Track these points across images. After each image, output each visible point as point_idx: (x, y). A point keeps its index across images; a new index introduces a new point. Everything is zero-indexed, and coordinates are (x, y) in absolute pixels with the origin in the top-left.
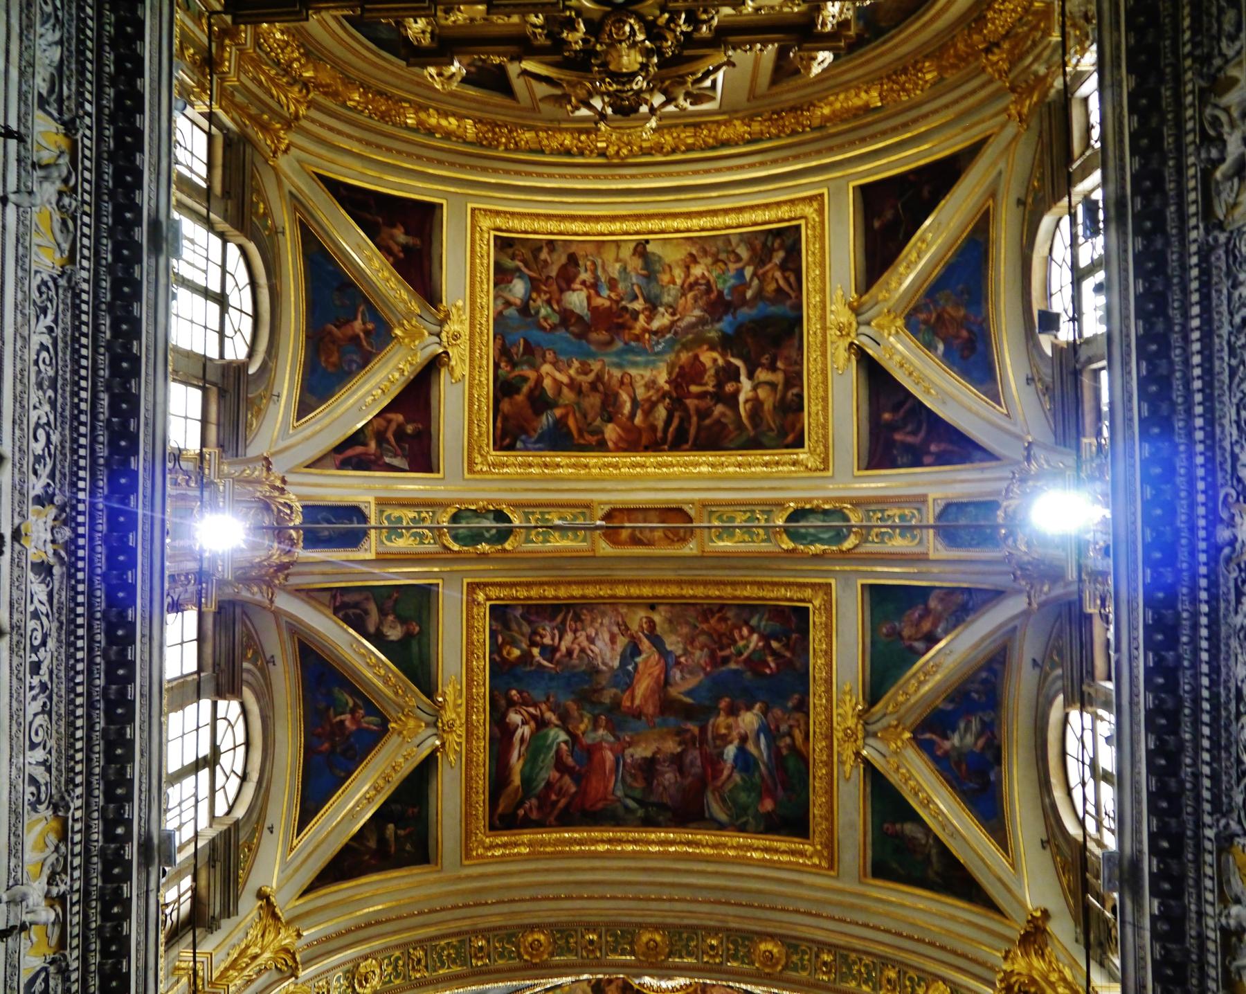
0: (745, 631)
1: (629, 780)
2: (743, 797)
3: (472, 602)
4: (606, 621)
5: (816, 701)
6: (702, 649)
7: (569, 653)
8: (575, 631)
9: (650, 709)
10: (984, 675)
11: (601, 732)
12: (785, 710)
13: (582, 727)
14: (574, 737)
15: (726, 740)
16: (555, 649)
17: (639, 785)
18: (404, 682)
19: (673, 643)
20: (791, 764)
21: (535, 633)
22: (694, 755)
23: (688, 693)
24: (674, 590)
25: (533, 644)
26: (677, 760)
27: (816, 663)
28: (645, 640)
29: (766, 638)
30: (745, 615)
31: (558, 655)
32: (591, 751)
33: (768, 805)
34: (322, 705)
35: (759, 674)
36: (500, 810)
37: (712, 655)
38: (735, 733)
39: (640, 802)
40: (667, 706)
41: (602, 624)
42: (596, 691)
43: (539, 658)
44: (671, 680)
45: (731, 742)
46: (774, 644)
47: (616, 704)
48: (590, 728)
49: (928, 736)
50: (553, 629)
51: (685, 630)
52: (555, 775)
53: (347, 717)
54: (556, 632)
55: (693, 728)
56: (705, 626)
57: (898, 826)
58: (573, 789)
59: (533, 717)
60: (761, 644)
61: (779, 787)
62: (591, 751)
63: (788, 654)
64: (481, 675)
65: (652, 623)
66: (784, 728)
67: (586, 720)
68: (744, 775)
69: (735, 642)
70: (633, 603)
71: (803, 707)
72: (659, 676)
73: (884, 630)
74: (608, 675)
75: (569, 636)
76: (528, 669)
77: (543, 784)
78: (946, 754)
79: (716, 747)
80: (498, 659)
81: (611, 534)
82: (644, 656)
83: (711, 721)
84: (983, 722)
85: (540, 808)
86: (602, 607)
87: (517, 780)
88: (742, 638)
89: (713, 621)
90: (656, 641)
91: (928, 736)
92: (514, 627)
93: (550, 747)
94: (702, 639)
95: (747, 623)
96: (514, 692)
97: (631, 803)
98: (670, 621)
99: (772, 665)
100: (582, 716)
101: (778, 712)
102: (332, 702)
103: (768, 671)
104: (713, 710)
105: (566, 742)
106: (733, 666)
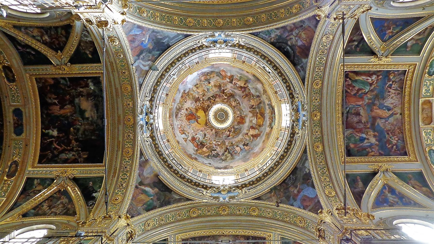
0: (397, 139)
1: (354, 109)
2: (353, 139)
3: (411, 65)
4: (397, 102)
5: (385, 158)
6: (390, 128)
7: (389, 92)
8: (395, 93)
9: (373, 114)
10: (412, 202)
11: (367, 101)
12: (378, 150)
13: (369, 96)
14: (367, 93)
15: (367, 134)
16: (390, 88)
17: (353, 111)
18: (397, 46)
19: (391, 120)
20: (364, 152)
21: (396, 82)
22: (362, 126)
23: (378, 123)
24: (407, 119)
25: (393, 82)
26: (360, 122)
27: (392, 158)
28: (392, 112)
29: (396, 145)
30: (401, 139)
31: (389, 89)
32: (362, 98)
33: (352, 146)
34: (398, 24)
35: (386, 143)
36: (350, 74)
37: (389, 130)
38: (369, 137)
39: (348, 112)
40: (374, 119)
41: (396, 100)
42: (378, 99)
43: (389, 83)
44: (381, 119)
45: (366, 136)
46: (395, 147)
47: (374, 105)
48: (368, 98)
49: (387, 187)
50: (396, 87)
51: (395, 123)
52: (357, 88)
53: (391, 30)
54: (395, 88)
55: (369, 126)
56: (396, 128)
57: (360, 180)
58: (352, 94)
59: (373, 82)
60: (394, 143)
61: (357, 149)
62: (362, 98)
63: (393, 150)
64: (389, 68)
65: (397, 114)
66: (373, 150)
67: (370, 97)
68: (358, 140)
69: (393, 136)
70: (403, 109)
71: (381, 155)
72: (382, 116)
73: (410, 176)
74: (382, 102)
75: (394, 92)
76: (386, 81)
77: (354, 85)
78: (384, 193)
79: (365, 132)
80: (391, 72)
81: (424, 103)
82: (388, 112)
83: (371, 130)
84: (397, 202)
85: (348, 85)
86: (401, 101)
87: (357, 78)
88: (394, 138)
89: (398, 130)
90: (392, 115)
91: (387, 187)
92: (398, 77)
93: (364, 87)
94: (393, 128)
95: (399, 139)
96: (381, 77)
97: (348, 109)
98: (397, 119)
99: (389, 146)
100: (372, 95)
101: (377, 148)
102: (397, 26)
103: (387, 145)
104: (374, 131)
105: (365, 91)
106: (387, 136)
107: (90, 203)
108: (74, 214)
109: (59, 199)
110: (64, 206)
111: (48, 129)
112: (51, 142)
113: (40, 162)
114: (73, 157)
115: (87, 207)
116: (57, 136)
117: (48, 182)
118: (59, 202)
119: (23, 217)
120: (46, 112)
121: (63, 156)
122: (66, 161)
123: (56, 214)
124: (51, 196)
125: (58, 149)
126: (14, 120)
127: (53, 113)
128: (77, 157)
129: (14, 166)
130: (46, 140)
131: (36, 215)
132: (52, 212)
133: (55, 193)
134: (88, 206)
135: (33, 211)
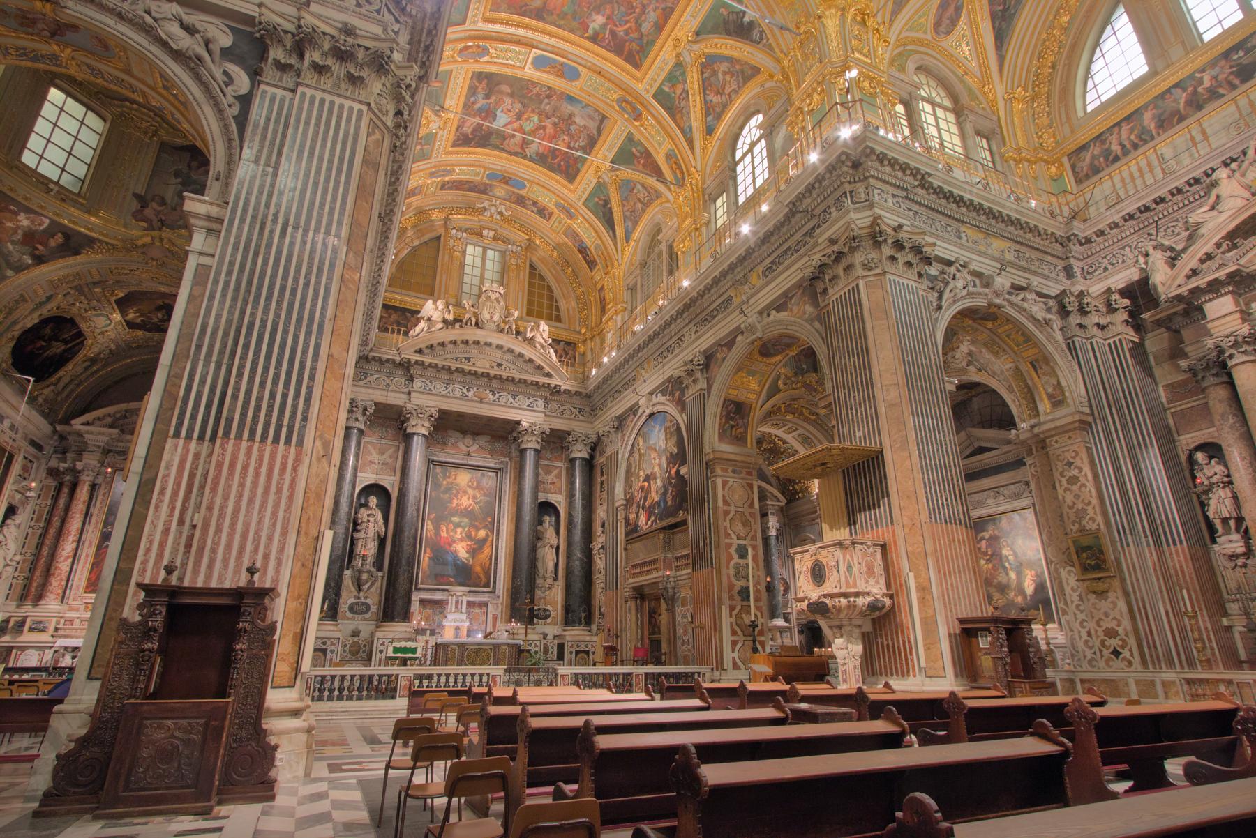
107: (755, 34)
108: (756, 71)
109: (714, 73)
110: (732, 75)
111: (588, 27)
112: (613, 33)
113: (637, 66)
114: (659, 12)
115: (760, 46)
116: (609, 18)
117: (678, 73)
118: (721, 76)
119: (710, 135)
120: (555, 17)
121: (646, 27)
122: (659, 27)
123: (736, 91)
124: (703, 82)
125: (630, 28)
126: (550, 72)
127: (563, 6)
128: (663, 6)
129: (624, 104)
130: (603, 38)
131: (719, 117)
132: (729, 94)
133: (702, 73)
134: (759, 43)
135: (708, 119)
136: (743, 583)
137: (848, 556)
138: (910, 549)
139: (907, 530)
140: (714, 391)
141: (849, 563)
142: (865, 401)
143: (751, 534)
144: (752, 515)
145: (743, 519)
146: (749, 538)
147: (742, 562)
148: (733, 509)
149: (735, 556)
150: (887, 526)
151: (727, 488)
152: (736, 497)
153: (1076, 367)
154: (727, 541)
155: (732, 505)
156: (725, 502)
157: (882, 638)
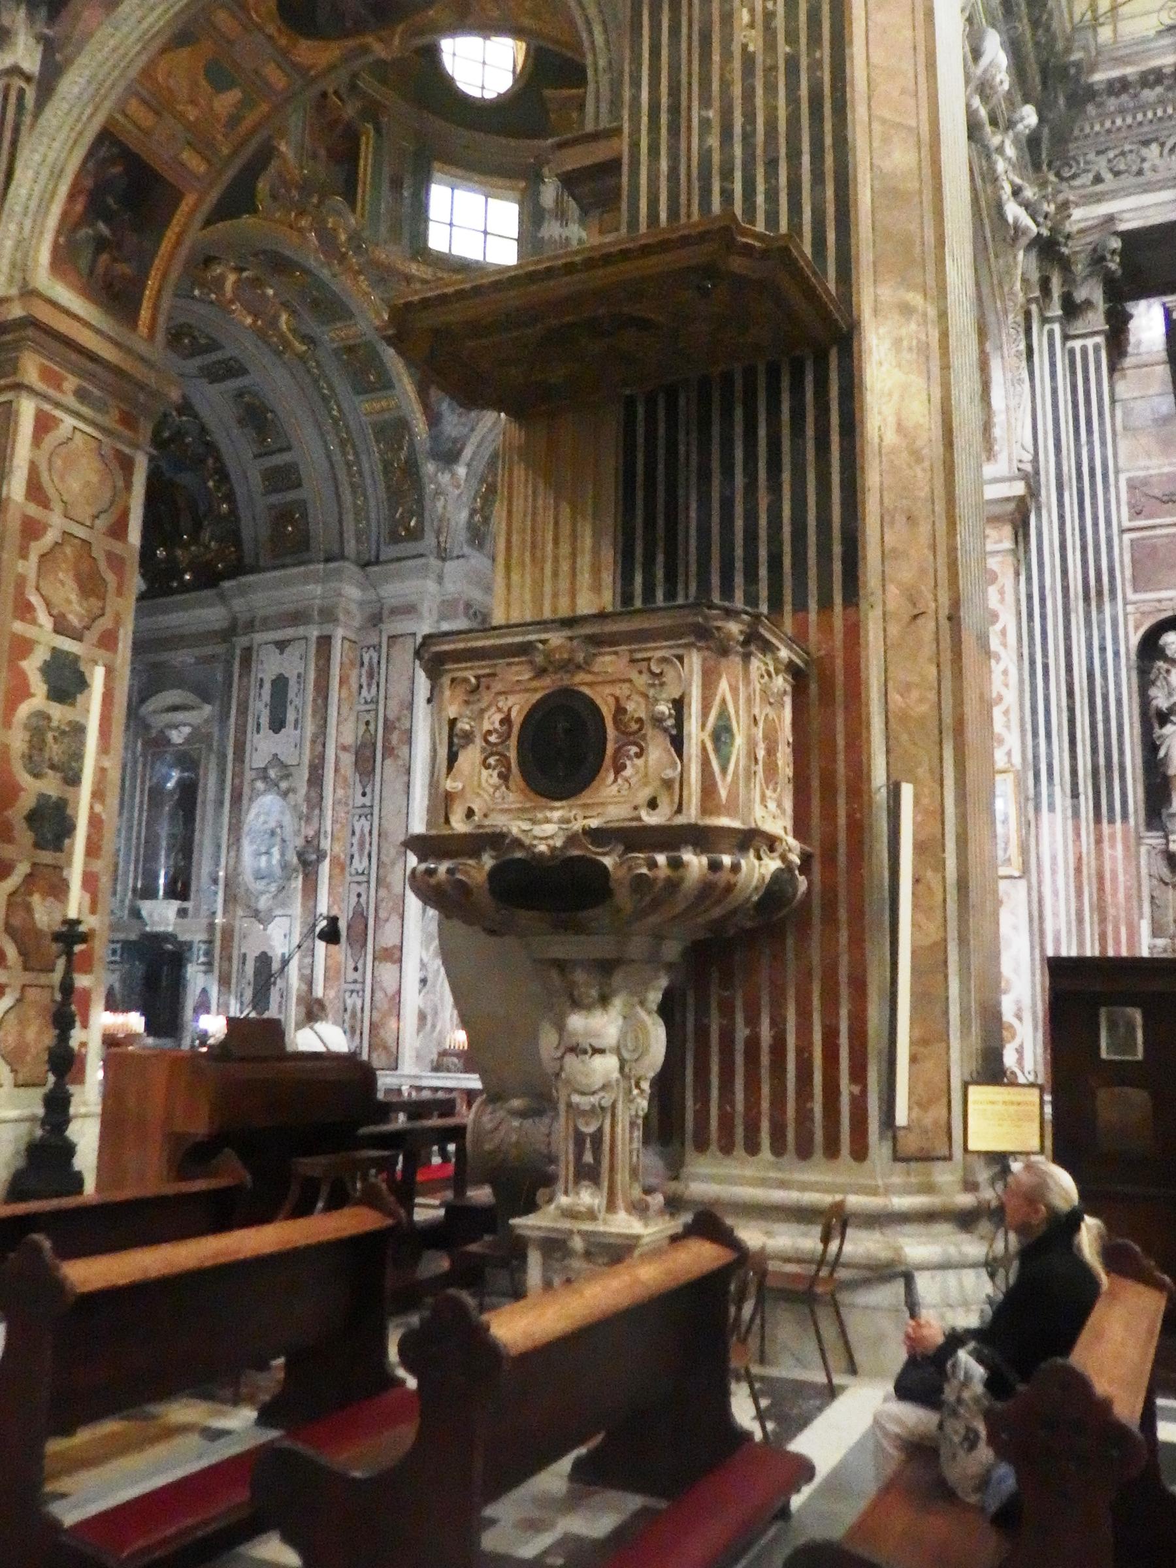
136: (50, 786)
137: (724, 686)
138: (895, 698)
139: (894, 630)
140: (72, 85)
141: (723, 714)
142: (794, 155)
143: (105, 623)
144: (117, 563)
145: (85, 567)
146: (92, 636)
147: (57, 712)
148: (56, 522)
149: (39, 687)
150: (825, 604)
151: (50, 440)
152: (74, 485)
153: (1025, 375)
154: (18, 627)
155: (58, 507)
156: (35, 490)
157: (727, 1010)
